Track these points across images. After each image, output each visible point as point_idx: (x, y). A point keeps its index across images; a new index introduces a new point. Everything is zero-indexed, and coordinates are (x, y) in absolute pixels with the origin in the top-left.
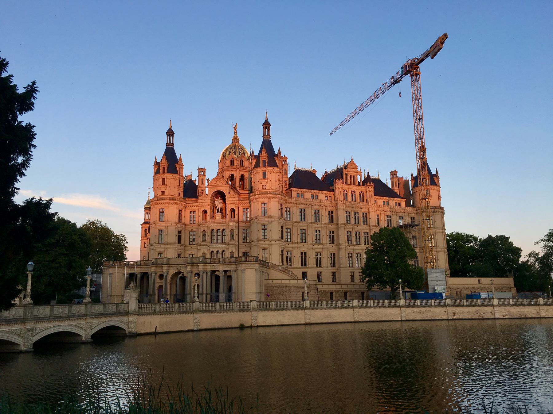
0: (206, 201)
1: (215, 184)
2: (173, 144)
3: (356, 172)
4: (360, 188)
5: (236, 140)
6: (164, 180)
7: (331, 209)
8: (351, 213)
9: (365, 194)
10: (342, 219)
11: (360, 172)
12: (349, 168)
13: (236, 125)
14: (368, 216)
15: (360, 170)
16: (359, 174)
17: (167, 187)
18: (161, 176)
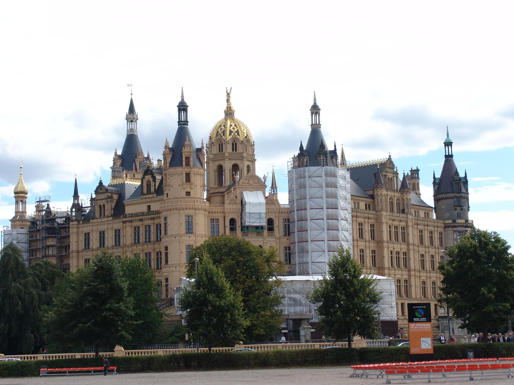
0: (235, 206)
1: (247, 184)
2: (186, 122)
3: (393, 173)
4: (396, 194)
5: (229, 113)
6: (188, 176)
7: (371, 221)
8: (391, 227)
9: (401, 201)
10: (385, 237)
11: (396, 174)
12: (388, 168)
13: (231, 90)
14: (405, 231)
15: (396, 170)
16: (396, 175)
17: (193, 185)
18: (183, 170)
